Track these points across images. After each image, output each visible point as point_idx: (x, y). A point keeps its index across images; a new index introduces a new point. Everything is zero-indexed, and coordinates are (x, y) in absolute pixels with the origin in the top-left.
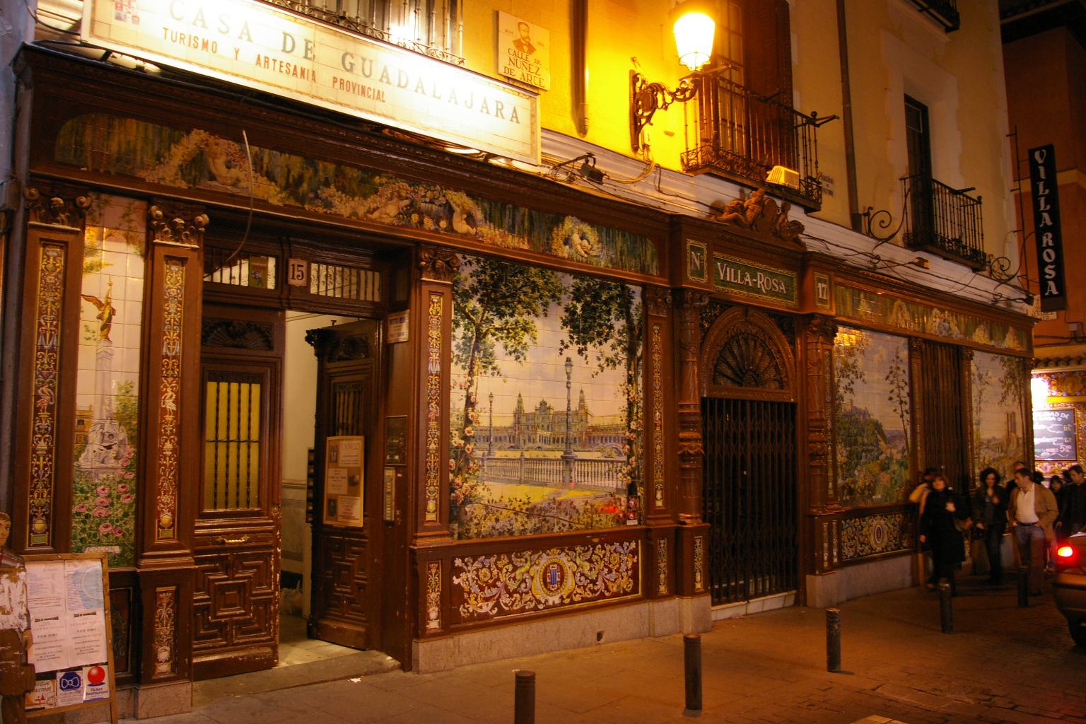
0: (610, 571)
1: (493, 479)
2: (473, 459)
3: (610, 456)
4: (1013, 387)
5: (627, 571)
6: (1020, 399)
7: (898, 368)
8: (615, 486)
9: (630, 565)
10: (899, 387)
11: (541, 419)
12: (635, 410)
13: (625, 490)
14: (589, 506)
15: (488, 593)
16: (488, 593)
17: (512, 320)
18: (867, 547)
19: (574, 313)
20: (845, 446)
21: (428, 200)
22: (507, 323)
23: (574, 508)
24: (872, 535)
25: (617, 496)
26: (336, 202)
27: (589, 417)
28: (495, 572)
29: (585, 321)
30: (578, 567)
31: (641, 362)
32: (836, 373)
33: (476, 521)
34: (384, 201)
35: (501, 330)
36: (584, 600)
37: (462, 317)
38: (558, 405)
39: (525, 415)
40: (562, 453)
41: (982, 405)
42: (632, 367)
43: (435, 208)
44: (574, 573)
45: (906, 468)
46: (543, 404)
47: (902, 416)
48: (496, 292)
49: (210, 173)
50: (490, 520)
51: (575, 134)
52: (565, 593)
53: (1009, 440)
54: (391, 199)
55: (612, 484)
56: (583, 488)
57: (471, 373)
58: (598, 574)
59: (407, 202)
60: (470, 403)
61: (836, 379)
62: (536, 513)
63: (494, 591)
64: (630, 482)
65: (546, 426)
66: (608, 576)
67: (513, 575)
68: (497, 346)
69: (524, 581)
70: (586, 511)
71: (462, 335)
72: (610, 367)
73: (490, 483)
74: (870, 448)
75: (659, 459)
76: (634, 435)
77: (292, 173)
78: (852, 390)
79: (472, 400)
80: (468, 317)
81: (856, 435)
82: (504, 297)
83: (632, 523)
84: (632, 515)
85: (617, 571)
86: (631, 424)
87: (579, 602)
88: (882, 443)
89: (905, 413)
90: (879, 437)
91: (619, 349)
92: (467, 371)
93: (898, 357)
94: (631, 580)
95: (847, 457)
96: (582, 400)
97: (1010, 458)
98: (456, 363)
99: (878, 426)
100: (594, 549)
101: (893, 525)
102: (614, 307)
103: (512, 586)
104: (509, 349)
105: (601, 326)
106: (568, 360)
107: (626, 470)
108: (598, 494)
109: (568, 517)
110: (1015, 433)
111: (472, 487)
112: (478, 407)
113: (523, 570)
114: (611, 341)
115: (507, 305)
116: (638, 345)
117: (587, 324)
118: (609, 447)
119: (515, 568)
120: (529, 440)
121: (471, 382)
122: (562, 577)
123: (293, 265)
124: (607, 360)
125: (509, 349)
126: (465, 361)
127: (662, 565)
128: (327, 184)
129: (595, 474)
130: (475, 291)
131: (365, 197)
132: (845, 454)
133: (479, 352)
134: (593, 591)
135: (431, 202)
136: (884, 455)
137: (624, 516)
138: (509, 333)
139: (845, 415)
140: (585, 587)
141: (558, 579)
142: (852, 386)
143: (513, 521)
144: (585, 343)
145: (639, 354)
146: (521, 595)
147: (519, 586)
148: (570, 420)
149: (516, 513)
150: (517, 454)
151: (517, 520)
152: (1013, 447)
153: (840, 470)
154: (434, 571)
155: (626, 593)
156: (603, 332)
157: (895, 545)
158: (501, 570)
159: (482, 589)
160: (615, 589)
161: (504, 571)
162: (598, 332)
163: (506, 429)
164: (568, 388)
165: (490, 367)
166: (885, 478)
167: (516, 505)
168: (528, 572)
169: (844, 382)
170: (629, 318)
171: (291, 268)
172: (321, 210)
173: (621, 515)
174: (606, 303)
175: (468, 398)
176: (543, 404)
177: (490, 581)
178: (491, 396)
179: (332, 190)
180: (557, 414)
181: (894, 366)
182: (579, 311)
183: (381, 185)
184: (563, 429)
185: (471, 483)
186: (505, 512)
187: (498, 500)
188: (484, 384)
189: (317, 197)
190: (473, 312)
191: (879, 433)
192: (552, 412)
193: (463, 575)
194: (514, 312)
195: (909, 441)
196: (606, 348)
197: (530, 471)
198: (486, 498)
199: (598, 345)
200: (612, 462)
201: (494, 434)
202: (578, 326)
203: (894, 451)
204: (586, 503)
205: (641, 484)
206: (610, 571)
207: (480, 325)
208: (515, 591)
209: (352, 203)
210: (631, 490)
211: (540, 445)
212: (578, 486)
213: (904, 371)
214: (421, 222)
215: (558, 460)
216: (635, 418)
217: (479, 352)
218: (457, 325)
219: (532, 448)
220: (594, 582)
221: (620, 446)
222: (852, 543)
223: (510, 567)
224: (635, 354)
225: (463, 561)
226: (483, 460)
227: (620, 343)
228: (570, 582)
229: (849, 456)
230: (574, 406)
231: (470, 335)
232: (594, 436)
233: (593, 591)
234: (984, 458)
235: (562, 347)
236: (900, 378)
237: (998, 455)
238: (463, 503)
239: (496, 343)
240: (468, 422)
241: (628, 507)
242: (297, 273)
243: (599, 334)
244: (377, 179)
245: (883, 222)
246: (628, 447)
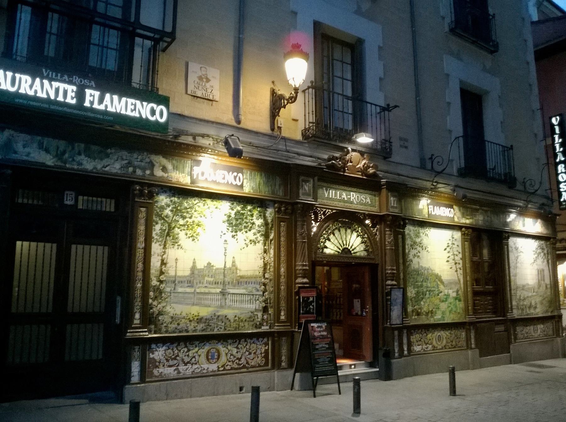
0: (250, 354)
1: (176, 303)
2: (165, 292)
3: (251, 292)
4: (542, 254)
5: (261, 354)
6: (548, 261)
8: (254, 308)
9: (263, 351)
10: (454, 255)
11: (207, 272)
12: (268, 267)
13: (261, 310)
14: (237, 318)
15: (171, 363)
16: (171, 363)
17: (190, 221)
18: (431, 346)
19: (230, 216)
20: (414, 288)
21: (139, 160)
22: (187, 222)
23: (228, 319)
24: (434, 339)
25: (255, 313)
26: (85, 162)
27: (238, 271)
28: (176, 352)
29: (237, 220)
30: (229, 351)
31: (273, 242)
32: (407, 247)
33: (165, 325)
34: (112, 161)
35: (184, 225)
36: (232, 369)
37: (160, 219)
38: (218, 264)
39: (197, 269)
40: (220, 290)
42: (267, 244)
43: (143, 164)
44: (227, 354)
45: (460, 300)
46: (209, 264)
48: (181, 206)
49: (14, 150)
50: (174, 324)
51: (235, 124)
52: (220, 363)
54: (117, 160)
55: (252, 307)
56: (234, 309)
57: (165, 247)
58: (242, 355)
59: (126, 162)
60: (163, 263)
61: (407, 251)
62: (203, 321)
63: (175, 362)
64: (264, 305)
65: (210, 275)
66: (248, 356)
67: (187, 354)
68: (182, 235)
69: (194, 357)
70: (235, 321)
71: (159, 228)
72: (252, 244)
73: (175, 305)
74: (433, 289)
75: (283, 294)
76: (267, 281)
77: (60, 149)
78: (419, 256)
79: (165, 262)
80: (164, 219)
81: (422, 282)
82: (186, 208)
83: (265, 328)
84: (265, 324)
85: (255, 353)
86: (266, 275)
87: (229, 370)
89: (458, 270)
90: (439, 283)
91: (258, 235)
92: (162, 247)
93: (453, 238)
94: (263, 359)
95: (415, 294)
96: (234, 262)
98: (156, 243)
100: (240, 341)
102: (256, 213)
103: (187, 359)
104: (188, 235)
105: (247, 223)
106: (226, 241)
107: (261, 299)
108: (242, 312)
109: (223, 324)
110: (544, 280)
111: (163, 307)
112: (168, 265)
113: (194, 351)
114: (253, 231)
115: (187, 212)
116: (271, 233)
117: (238, 222)
118: (250, 287)
119: (189, 350)
120: (200, 283)
121: (165, 252)
122: (219, 356)
123: (67, 194)
124: (251, 241)
125: (188, 235)
126: (161, 241)
127: (284, 351)
128: (80, 154)
129: (242, 302)
130: (169, 206)
131: (102, 159)
132: (414, 292)
133: (170, 237)
134: (239, 364)
135: (141, 161)
136: (442, 294)
137: (260, 324)
138: (188, 227)
140: (233, 362)
141: (216, 357)
142: (419, 254)
143: (188, 325)
144: (236, 232)
145: (271, 237)
146: (192, 364)
147: (191, 360)
148: (226, 272)
149: (190, 321)
150: (192, 290)
151: (190, 324)
153: (410, 301)
154: (137, 350)
155: (260, 366)
156: (248, 226)
157: (452, 345)
158: (180, 351)
159: (168, 361)
160: (253, 364)
161: (182, 351)
162: (245, 226)
163: (185, 277)
164: (225, 256)
165: (176, 244)
166: (443, 306)
167: (190, 317)
168: (197, 352)
170: (265, 218)
171: (66, 195)
172: (76, 167)
173: (258, 323)
174: (250, 211)
175: (162, 260)
176: (209, 264)
177: (173, 357)
178: (177, 259)
179: (83, 157)
180: (217, 269)
181: (450, 243)
182: (233, 216)
183: (111, 153)
184: (222, 277)
185: (163, 304)
186: (183, 320)
187: (179, 314)
188: (172, 253)
189: (73, 160)
190: (167, 216)
191: (439, 280)
192: (214, 268)
193: (156, 353)
194: (192, 216)
195: (462, 286)
196: (250, 235)
197: (200, 299)
198: (172, 313)
199: (244, 233)
200: (253, 295)
201: (178, 279)
202: (232, 223)
204: (236, 316)
205: (271, 307)
206: (250, 354)
207: (171, 223)
208: (188, 362)
209: (94, 163)
210: (265, 310)
211: (206, 285)
212: (230, 307)
213: (458, 246)
214: (134, 172)
215: (217, 293)
216: (268, 271)
217: (170, 237)
218: (157, 223)
219: (201, 287)
220: (239, 359)
221: (258, 286)
223: (186, 350)
224: (269, 238)
225: (156, 346)
226: (170, 293)
227: (259, 232)
228: (223, 359)
230: (229, 265)
231: (164, 228)
233: (239, 364)
234: (520, 296)
235: (222, 234)
238: (157, 315)
239: (180, 232)
240: (162, 273)
241: (263, 319)
242: (68, 198)
243: (245, 227)
244: (109, 151)
245: (439, 162)
246: (263, 287)
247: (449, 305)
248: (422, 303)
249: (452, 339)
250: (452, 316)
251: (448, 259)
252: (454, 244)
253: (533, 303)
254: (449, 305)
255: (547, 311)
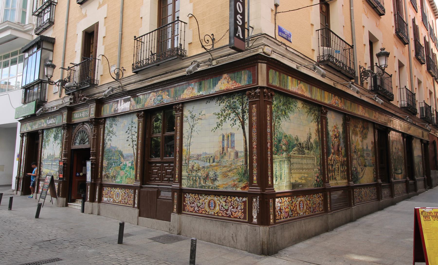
7: (133, 127)
41: (194, 134)
45: (133, 169)
47: (133, 147)
53: (223, 153)
56: (53, 170)
88: (122, 159)
97: (224, 167)
99: (121, 153)
101: (125, 193)
132: (106, 163)
136: (122, 164)
139: (108, 149)
152: (229, 159)
169: (108, 137)
181: (130, 126)
203: (127, 162)
213: (135, 127)
222: (107, 196)
229: (108, 164)
232: (55, 159)
234: (193, 166)
236: (133, 131)
237: (208, 164)
247: (126, 172)
248: (110, 170)
249: (125, 197)
250: (127, 180)
251: (128, 139)
252: (133, 127)
253: (211, 174)
254: (126, 172)
255: (235, 186)
